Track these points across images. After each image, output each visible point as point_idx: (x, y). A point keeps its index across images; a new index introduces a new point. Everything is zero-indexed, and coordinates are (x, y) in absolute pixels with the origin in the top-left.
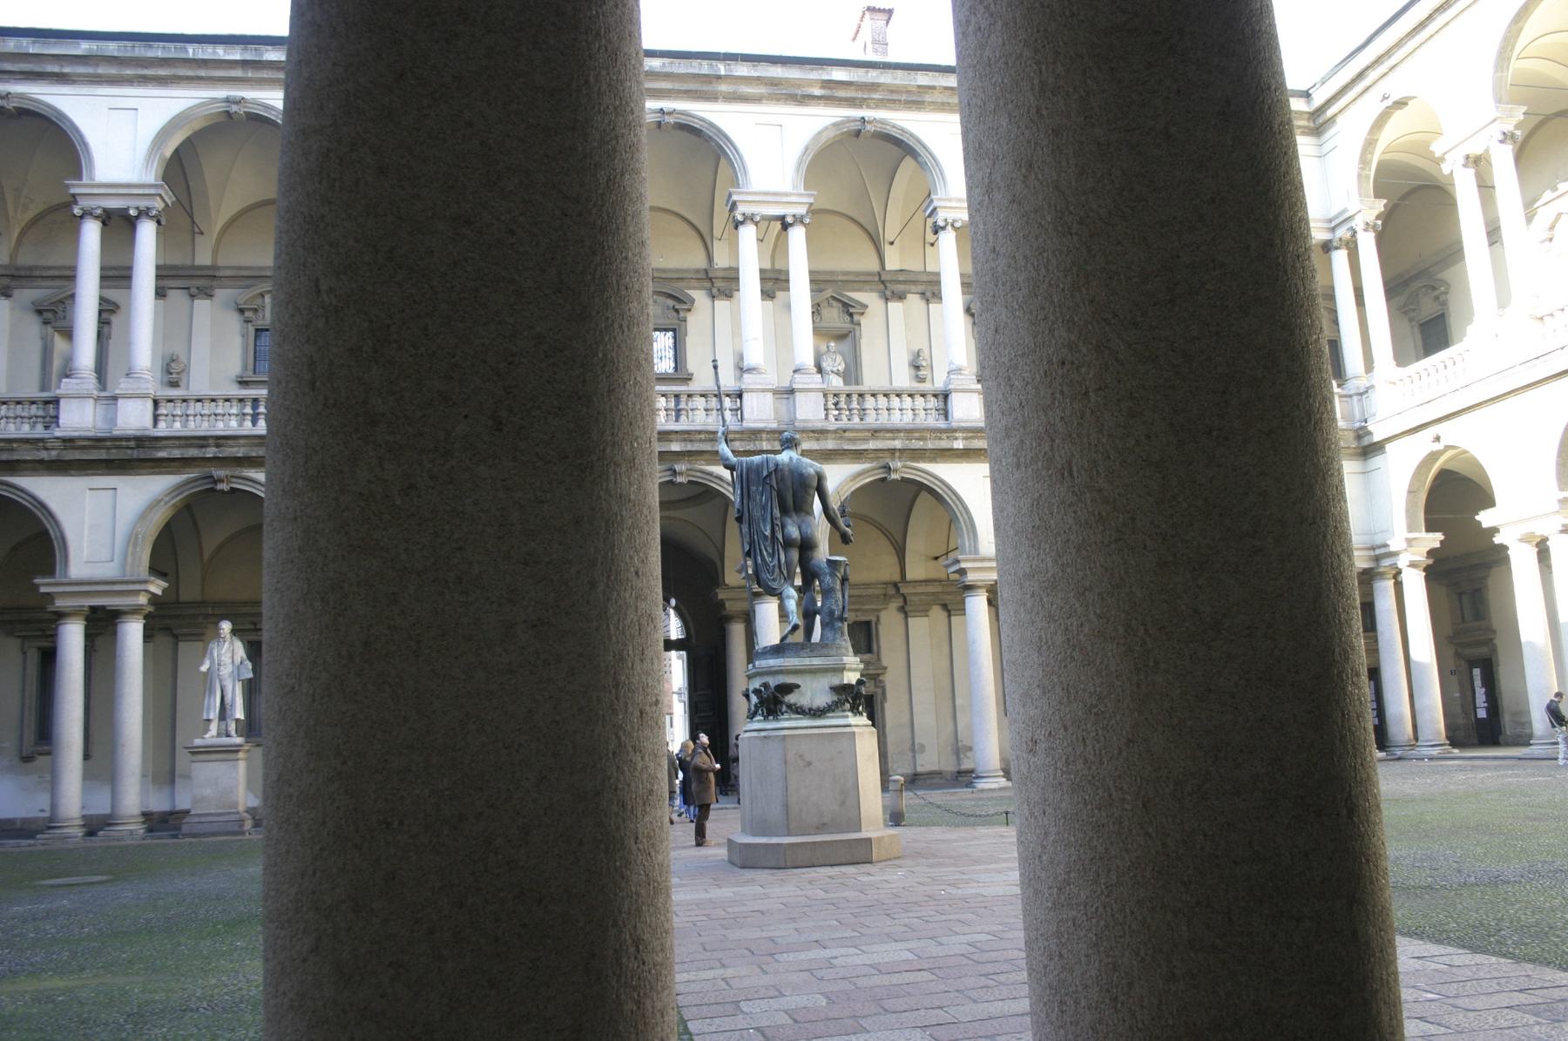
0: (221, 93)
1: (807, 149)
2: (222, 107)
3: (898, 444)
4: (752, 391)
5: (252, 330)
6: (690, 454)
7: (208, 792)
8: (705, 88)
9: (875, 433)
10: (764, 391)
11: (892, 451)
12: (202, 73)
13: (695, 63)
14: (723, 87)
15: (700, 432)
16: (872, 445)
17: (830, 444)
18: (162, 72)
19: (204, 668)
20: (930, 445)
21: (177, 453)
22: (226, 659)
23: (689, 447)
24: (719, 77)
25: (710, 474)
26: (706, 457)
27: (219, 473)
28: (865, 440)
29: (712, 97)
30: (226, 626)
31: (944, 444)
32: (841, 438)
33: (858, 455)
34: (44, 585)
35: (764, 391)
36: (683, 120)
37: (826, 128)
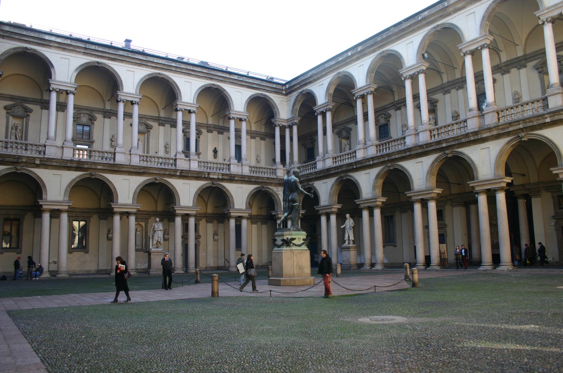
0: (335, 73)
1: (484, 17)
2: (336, 77)
3: (521, 126)
4: (469, 118)
5: (378, 127)
6: (451, 146)
7: (345, 259)
8: (445, 13)
9: (510, 124)
10: (473, 117)
11: (522, 130)
12: (331, 69)
13: (437, 6)
14: (450, 9)
15: (449, 138)
16: (511, 129)
17: (495, 132)
18: (324, 73)
19: (342, 227)
20: (535, 123)
21: (334, 172)
22: (348, 224)
23: (448, 144)
24: (447, 7)
25: (458, 152)
26: (456, 146)
27: (342, 175)
28: (508, 128)
29: (449, 14)
30: (348, 216)
31: (541, 121)
32: (498, 129)
33: (508, 134)
34: (357, 202)
35: (473, 117)
36: (443, 26)
37: (490, 5)
